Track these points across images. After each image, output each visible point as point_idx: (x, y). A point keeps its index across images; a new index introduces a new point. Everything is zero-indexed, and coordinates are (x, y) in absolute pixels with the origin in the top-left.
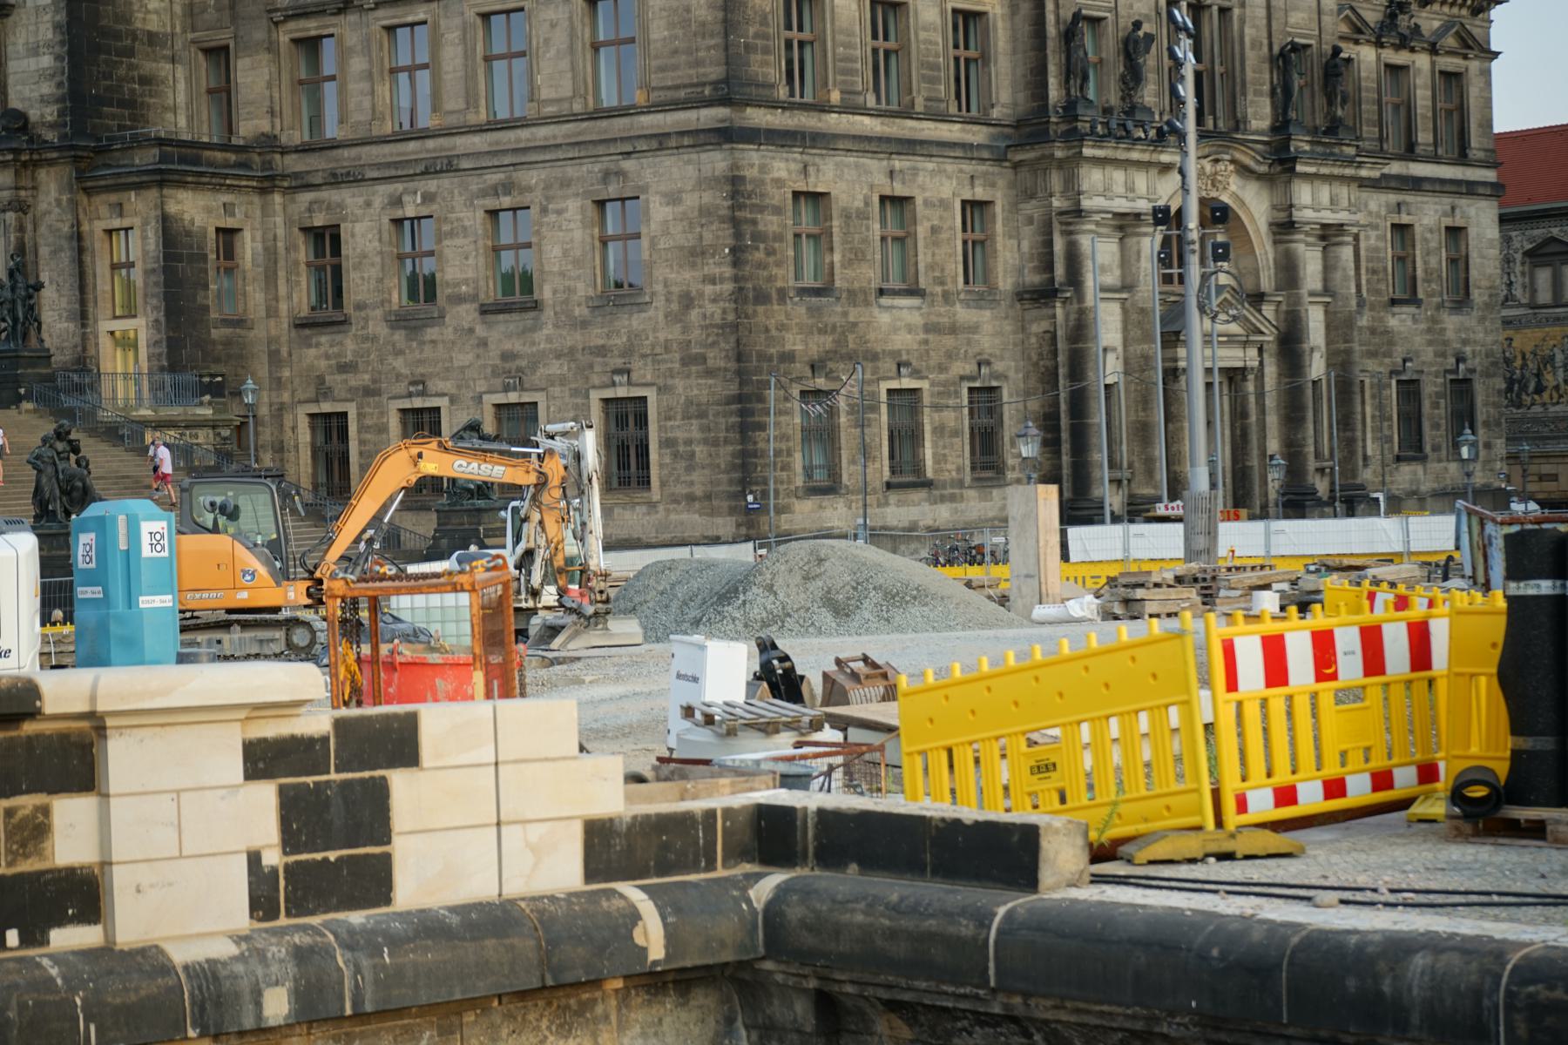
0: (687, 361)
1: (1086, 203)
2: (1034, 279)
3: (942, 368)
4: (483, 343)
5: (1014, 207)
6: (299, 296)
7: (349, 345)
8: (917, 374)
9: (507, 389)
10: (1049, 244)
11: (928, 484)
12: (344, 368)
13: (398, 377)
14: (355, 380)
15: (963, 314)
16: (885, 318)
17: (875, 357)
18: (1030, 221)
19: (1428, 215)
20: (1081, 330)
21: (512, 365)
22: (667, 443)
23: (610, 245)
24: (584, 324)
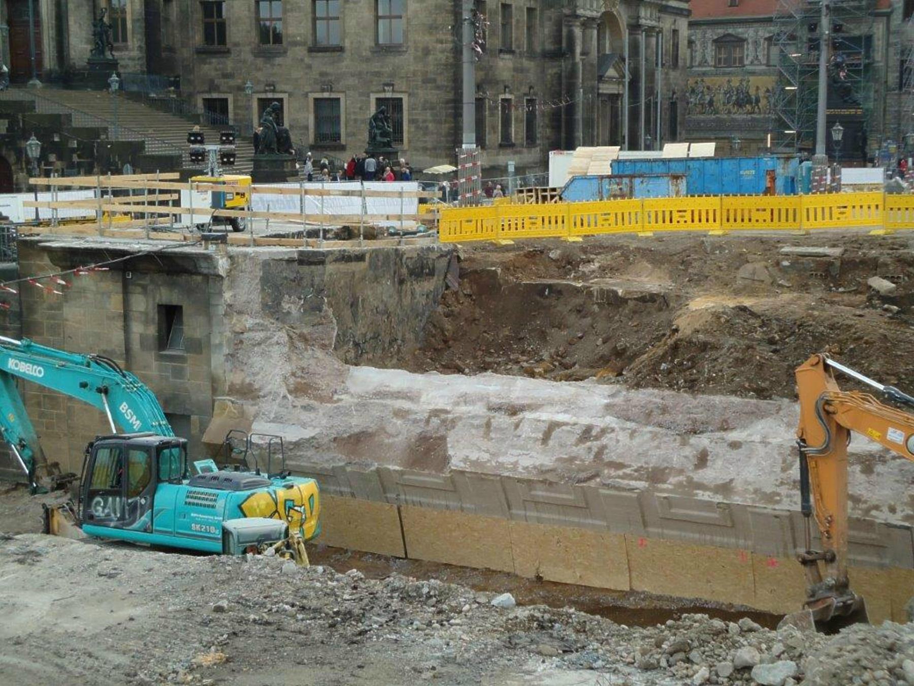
0: (426, 81)
1: (580, 12)
2: (549, 47)
3: (518, 90)
4: (309, 67)
5: (542, 11)
6: (198, 38)
7: (229, 64)
8: (511, 93)
9: (323, 91)
10: (560, 31)
11: (512, 145)
12: (226, 76)
13: (259, 82)
14: (232, 83)
15: (526, 63)
16: (501, 64)
17: (497, 83)
18: (550, 19)
19: (667, 23)
20: (572, 74)
21: (327, 79)
22: (412, 121)
23: (381, 22)
24: (368, 60)
